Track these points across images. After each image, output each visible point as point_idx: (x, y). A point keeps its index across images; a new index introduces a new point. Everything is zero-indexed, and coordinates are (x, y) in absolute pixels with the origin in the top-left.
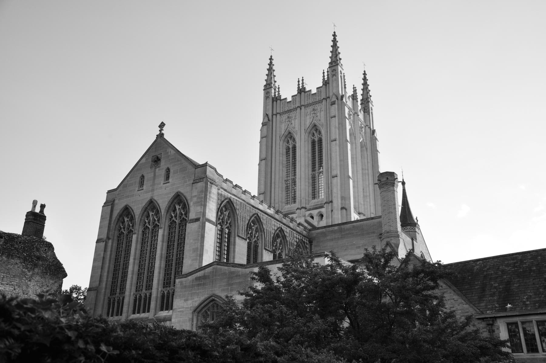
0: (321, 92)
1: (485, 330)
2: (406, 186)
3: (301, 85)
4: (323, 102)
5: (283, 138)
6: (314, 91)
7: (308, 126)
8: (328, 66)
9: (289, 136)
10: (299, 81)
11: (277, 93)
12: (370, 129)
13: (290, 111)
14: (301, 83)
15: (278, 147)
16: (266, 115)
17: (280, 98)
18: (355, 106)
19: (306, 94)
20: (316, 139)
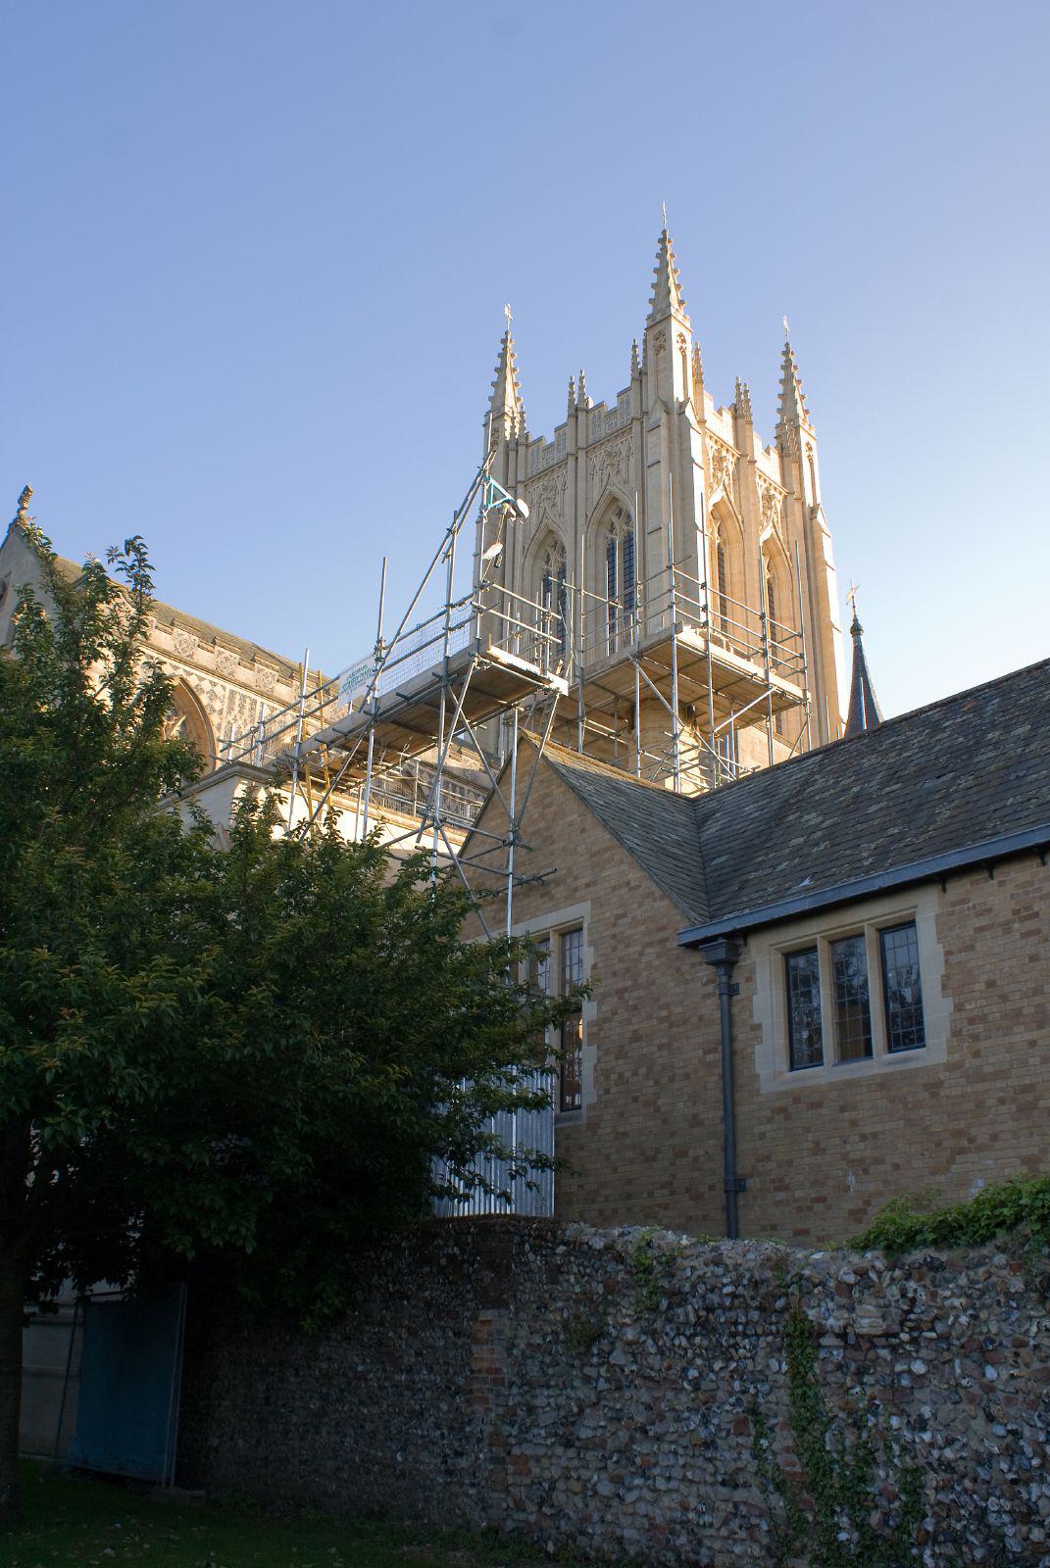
0: (628, 403)
1: (710, 988)
2: (863, 638)
4: (633, 430)
5: (533, 549)
6: (612, 403)
9: (550, 541)
12: (803, 503)
13: (549, 470)
15: (518, 573)
17: (527, 439)
18: (740, 438)
19: (591, 416)
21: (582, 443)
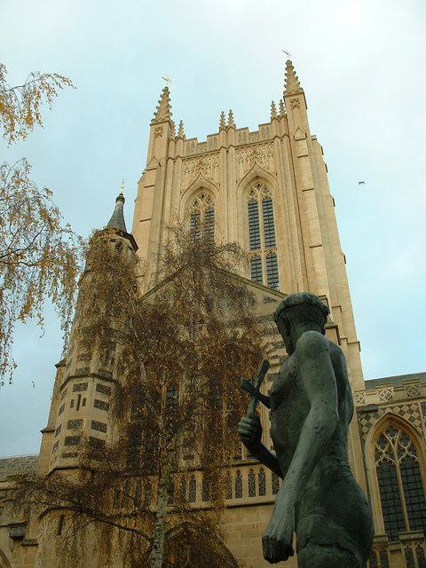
3: (227, 121)
5: (187, 195)
7: (242, 177)
10: (223, 116)
14: (227, 117)
20: (259, 200)
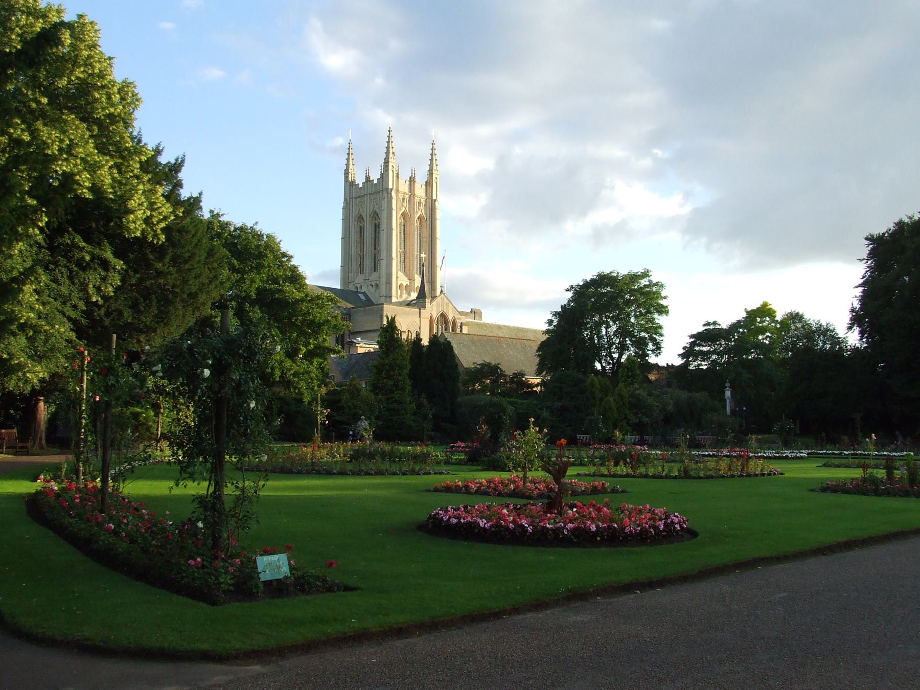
3: (367, 175)
6: (375, 182)
8: (383, 161)
11: (353, 178)
16: (345, 200)
20: (377, 223)
21: (368, 192)
